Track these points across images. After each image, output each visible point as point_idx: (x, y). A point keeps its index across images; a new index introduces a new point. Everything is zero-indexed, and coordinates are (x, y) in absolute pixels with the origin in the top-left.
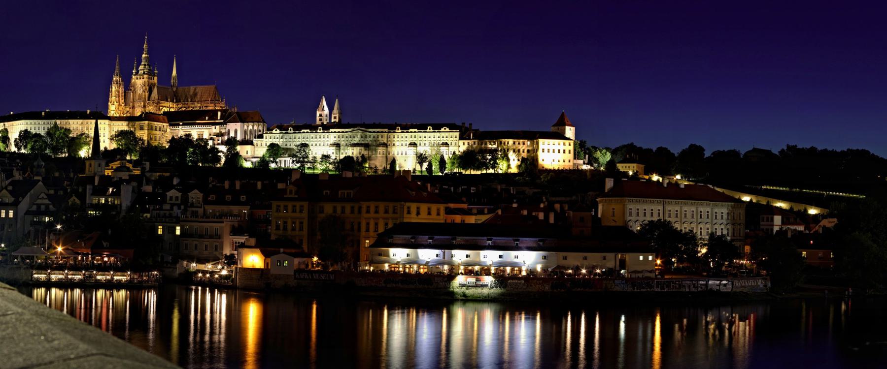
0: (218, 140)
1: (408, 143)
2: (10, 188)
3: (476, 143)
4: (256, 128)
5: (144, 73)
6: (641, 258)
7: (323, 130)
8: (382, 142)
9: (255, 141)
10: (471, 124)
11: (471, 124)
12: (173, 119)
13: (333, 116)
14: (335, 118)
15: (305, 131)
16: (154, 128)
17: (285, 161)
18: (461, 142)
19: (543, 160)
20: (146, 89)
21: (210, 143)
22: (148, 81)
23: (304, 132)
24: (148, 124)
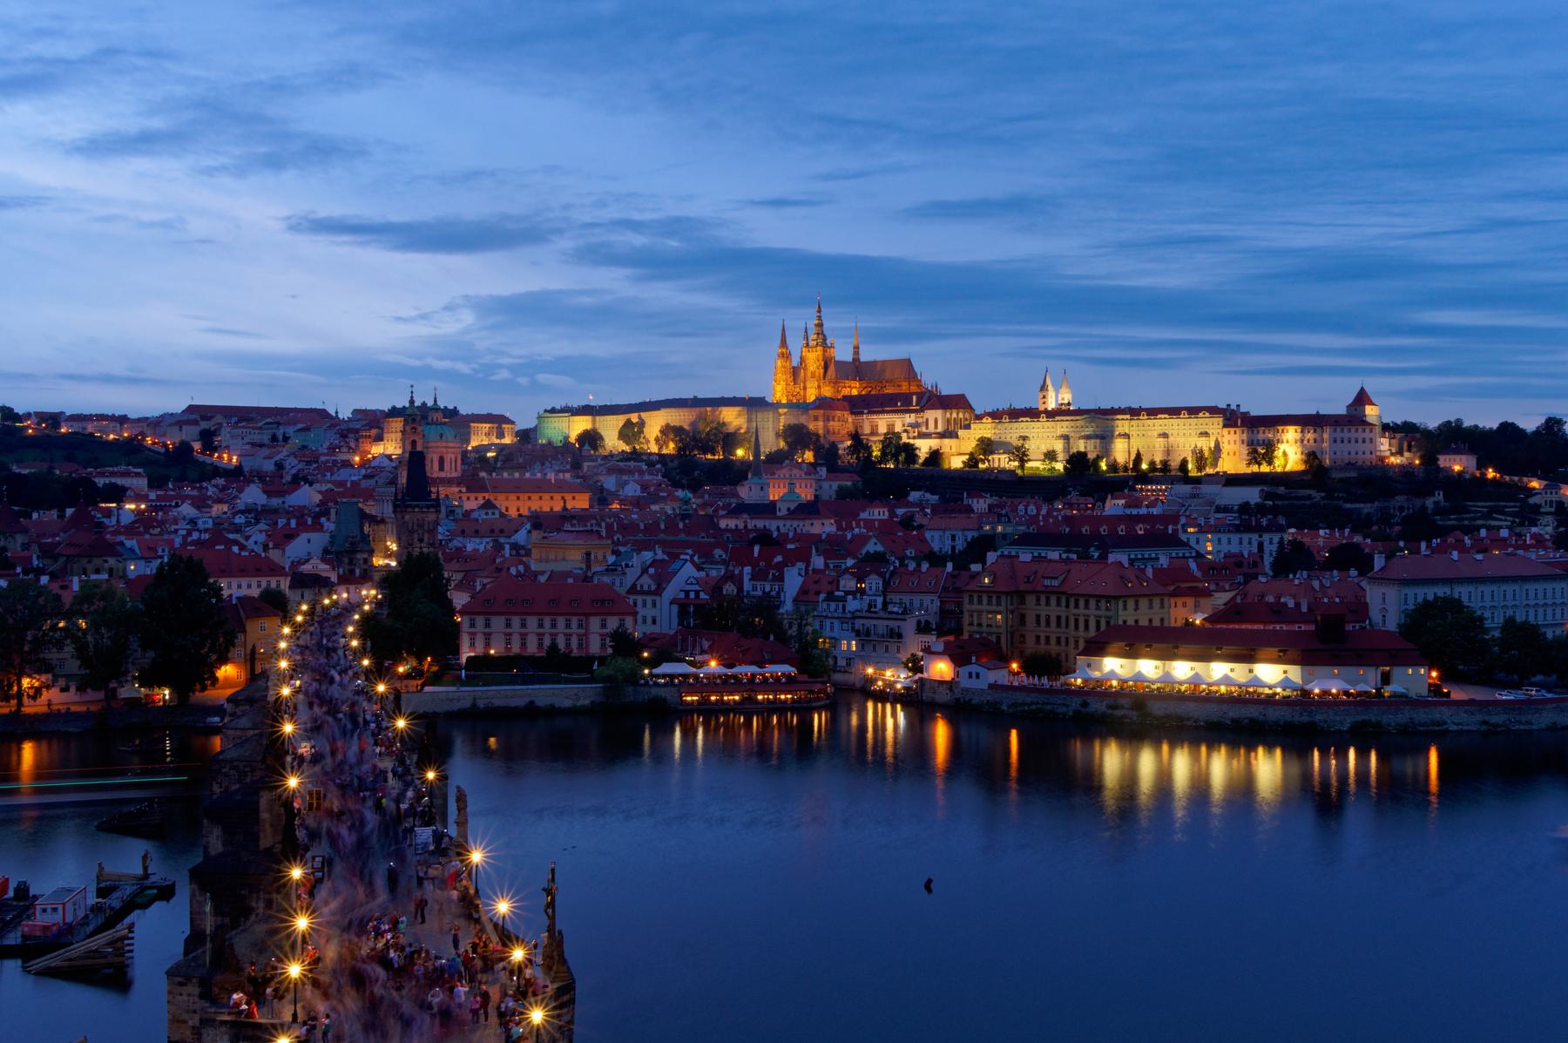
0: (914, 432)
1: (1156, 434)
2: (652, 571)
3: (1245, 431)
4: (961, 415)
5: (817, 344)
6: (1410, 671)
7: (1047, 417)
8: (1123, 432)
9: (961, 433)
11: (1238, 406)
12: (858, 405)
13: (1060, 397)
14: (1063, 399)
15: (1024, 419)
17: (999, 459)
18: (1226, 430)
20: (820, 365)
21: (904, 435)
22: (824, 354)
23: (1022, 421)
24: (824, 414)
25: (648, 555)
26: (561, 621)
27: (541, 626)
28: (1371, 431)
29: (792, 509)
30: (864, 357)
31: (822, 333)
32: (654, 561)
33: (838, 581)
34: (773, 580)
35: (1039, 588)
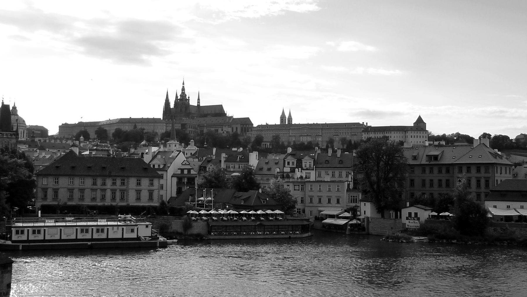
2: (159, 156)
3: (373, 133)
4: (247, 126)
5: (183, 98)
10: (367, 123)
11: (367, 123)
25: (154, 149)
26: (109, 182)
27: (95, 184)
28: (426, 133)
29: (193, 154)
30: (201, 105)
31: (185, 93)
32: (159, 151)
33: (284, 161)
34: (240, 162)
35: (424, 162)
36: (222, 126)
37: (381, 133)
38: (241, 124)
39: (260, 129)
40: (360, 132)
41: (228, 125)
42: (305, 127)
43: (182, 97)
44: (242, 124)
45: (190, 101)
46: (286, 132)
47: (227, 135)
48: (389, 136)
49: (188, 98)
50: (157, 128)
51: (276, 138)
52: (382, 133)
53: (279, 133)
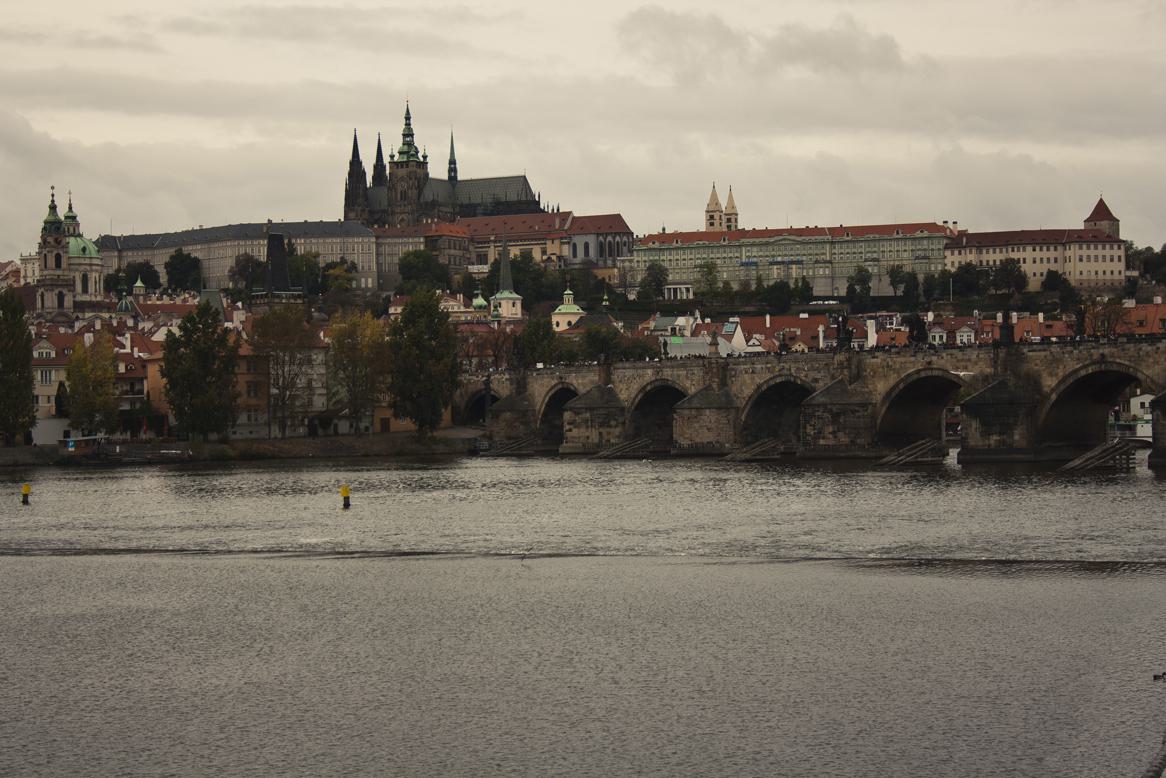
4: (618, 238)
5: (408, 157)
15: (701, 243)
16: (452, 245)
19: (1081, 273)
28: (1119, 248)
29: (573, 323)
36: (543, 239)
37: (998, 250)
38: (598, 235)
39: (657, 245)
40: (939, 249)
41: (562, 238)
42: (784, 239)
43: (405, 156)
44: (601, 234)
45: (429, 166)
46: (730, 255)
47: (560, 266)
48: (1019, 259)
49: (422, 159)
50: (354, 250)
51: (709, 269)
52: (1001, 252)
53: (712, 256)
